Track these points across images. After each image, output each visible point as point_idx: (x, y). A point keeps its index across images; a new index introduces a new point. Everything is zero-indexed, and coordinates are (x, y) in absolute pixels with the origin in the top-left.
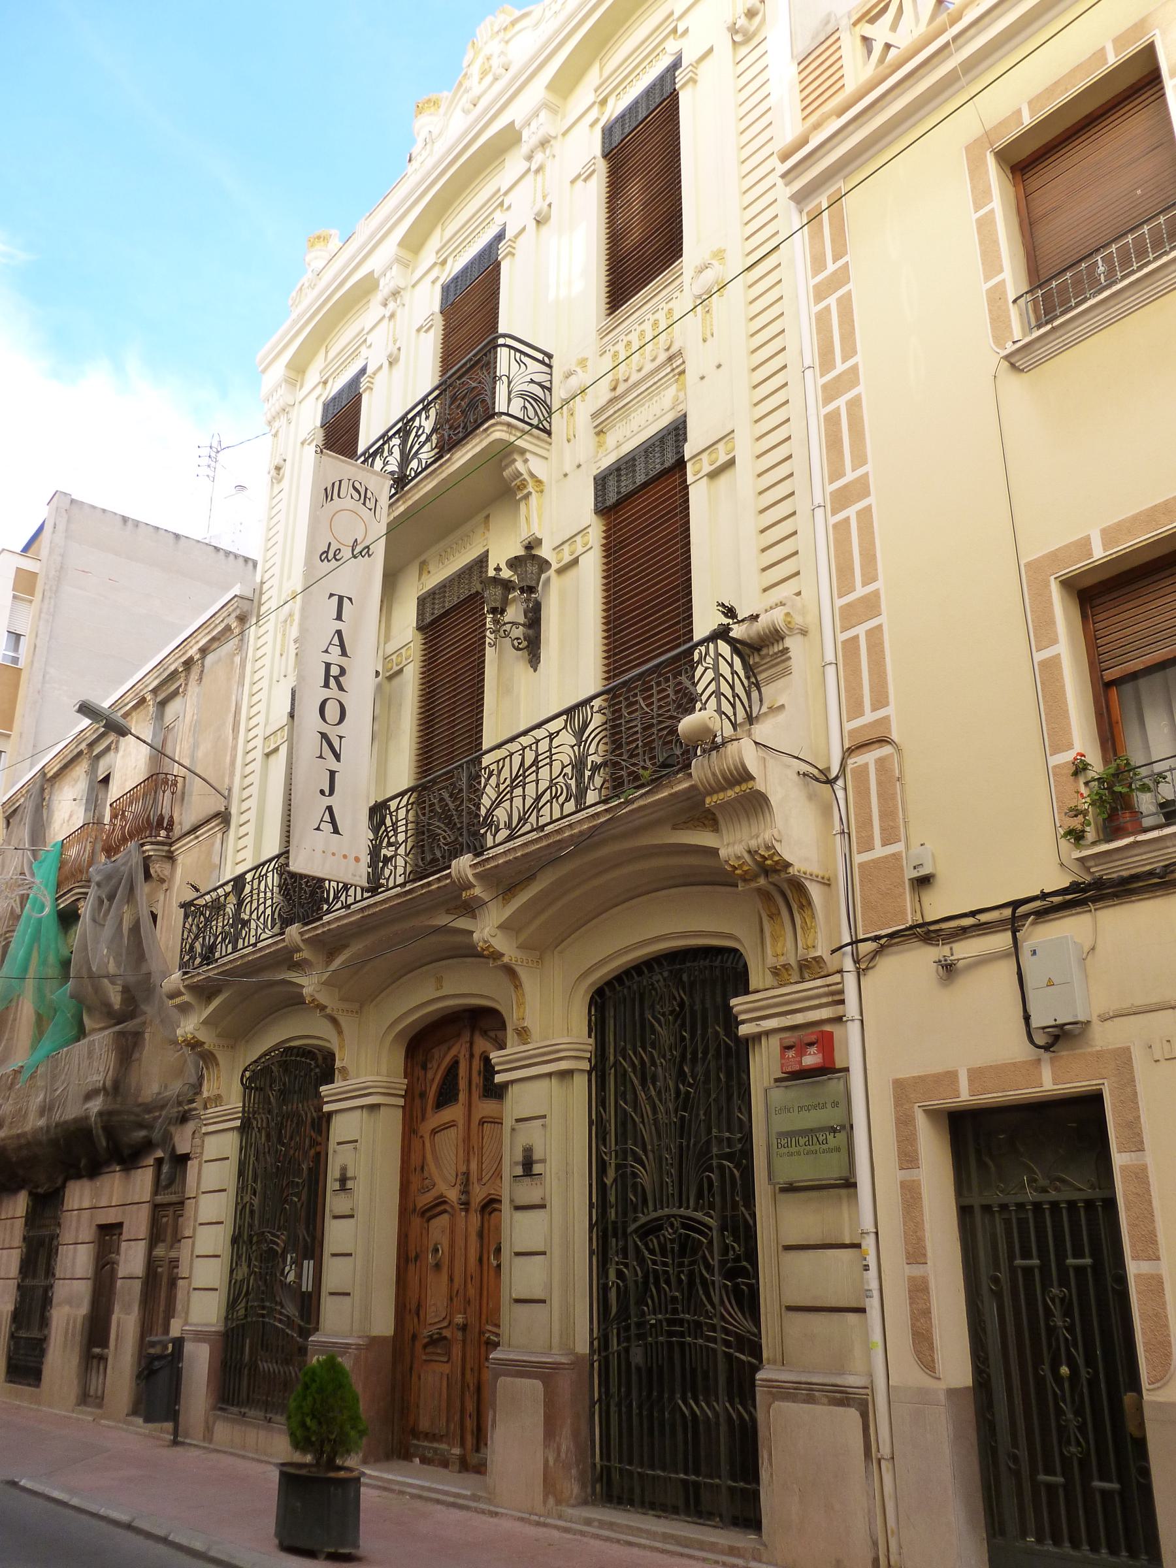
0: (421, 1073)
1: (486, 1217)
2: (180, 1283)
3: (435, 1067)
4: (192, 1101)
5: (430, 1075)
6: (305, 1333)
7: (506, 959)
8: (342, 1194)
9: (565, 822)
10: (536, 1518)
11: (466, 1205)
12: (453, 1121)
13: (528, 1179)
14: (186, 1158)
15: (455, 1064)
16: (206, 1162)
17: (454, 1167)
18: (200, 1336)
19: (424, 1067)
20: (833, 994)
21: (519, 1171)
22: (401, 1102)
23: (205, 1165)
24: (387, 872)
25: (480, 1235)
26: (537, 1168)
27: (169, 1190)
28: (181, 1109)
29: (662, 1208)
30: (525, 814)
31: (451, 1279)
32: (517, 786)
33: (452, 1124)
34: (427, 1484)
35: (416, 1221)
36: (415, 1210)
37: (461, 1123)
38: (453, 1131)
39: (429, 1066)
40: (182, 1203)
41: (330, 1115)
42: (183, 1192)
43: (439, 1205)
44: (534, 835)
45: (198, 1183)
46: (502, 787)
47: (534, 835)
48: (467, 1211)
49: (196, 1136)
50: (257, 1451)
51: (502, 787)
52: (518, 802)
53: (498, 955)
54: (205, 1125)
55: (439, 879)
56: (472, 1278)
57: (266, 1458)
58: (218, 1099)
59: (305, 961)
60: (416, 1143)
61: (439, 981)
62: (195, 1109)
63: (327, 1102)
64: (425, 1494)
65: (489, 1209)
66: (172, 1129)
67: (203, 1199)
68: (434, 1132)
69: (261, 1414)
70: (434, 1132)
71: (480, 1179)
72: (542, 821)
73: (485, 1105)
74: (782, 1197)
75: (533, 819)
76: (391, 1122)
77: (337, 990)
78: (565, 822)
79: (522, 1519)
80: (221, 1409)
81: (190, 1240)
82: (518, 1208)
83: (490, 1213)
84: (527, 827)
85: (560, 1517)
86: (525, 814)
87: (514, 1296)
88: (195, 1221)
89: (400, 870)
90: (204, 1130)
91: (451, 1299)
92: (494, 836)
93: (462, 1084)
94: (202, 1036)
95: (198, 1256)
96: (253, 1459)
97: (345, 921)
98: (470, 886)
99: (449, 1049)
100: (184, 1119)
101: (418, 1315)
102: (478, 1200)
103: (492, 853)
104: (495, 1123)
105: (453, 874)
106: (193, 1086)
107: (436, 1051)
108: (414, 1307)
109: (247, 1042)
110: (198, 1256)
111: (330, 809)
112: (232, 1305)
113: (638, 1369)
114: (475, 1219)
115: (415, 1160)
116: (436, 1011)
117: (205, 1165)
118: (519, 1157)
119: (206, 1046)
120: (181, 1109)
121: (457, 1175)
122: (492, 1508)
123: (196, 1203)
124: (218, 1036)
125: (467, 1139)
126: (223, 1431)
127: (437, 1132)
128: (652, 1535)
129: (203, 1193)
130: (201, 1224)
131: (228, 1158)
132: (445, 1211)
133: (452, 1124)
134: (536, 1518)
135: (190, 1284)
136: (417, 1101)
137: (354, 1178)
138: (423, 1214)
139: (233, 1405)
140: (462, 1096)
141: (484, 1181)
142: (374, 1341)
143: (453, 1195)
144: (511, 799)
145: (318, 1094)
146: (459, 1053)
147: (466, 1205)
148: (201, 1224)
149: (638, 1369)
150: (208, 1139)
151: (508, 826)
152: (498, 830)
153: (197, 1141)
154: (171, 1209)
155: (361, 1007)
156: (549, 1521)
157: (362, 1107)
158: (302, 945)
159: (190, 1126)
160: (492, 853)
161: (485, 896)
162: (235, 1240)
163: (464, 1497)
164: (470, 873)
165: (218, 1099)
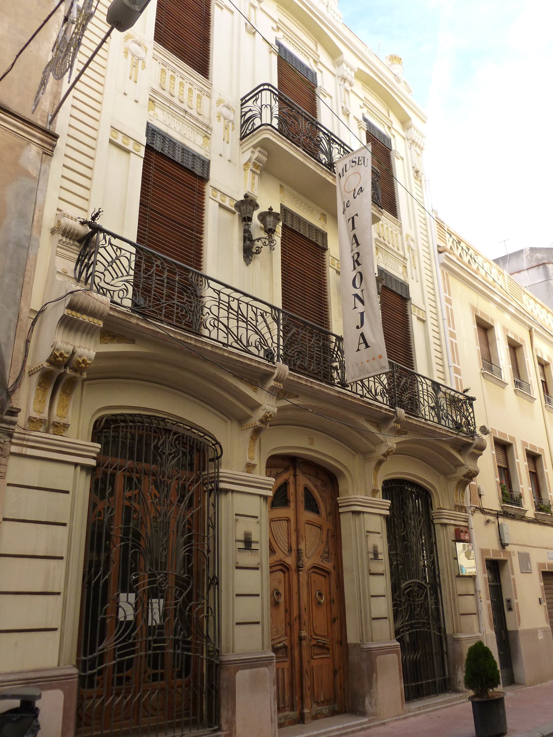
8: (248, 552)
10: (401, 716)
17: (287, 545)
20: (465, 519)
21: (372, 556)
26: (254, 546)
29: (409, 580)
34: (341, 726)
55: (306, 381)
56: (305, 610)
64: (344, 731)
74: (457, 578)
79: (396, 720)
82: (371, 574)
85: (409, 712)
87: (373, 616)
93: (292, 498)
111: (362, 335)
113: (408, 644)
118: (371, 549)
122: (382, 722)
128: (440, 703)
134: (401, 716)
137: (257, 542)
140: (292, 505)
146: (289, 478)
149: (408, 644)
156: (407, 715)
162: (215, 581)
163: (365, 723)
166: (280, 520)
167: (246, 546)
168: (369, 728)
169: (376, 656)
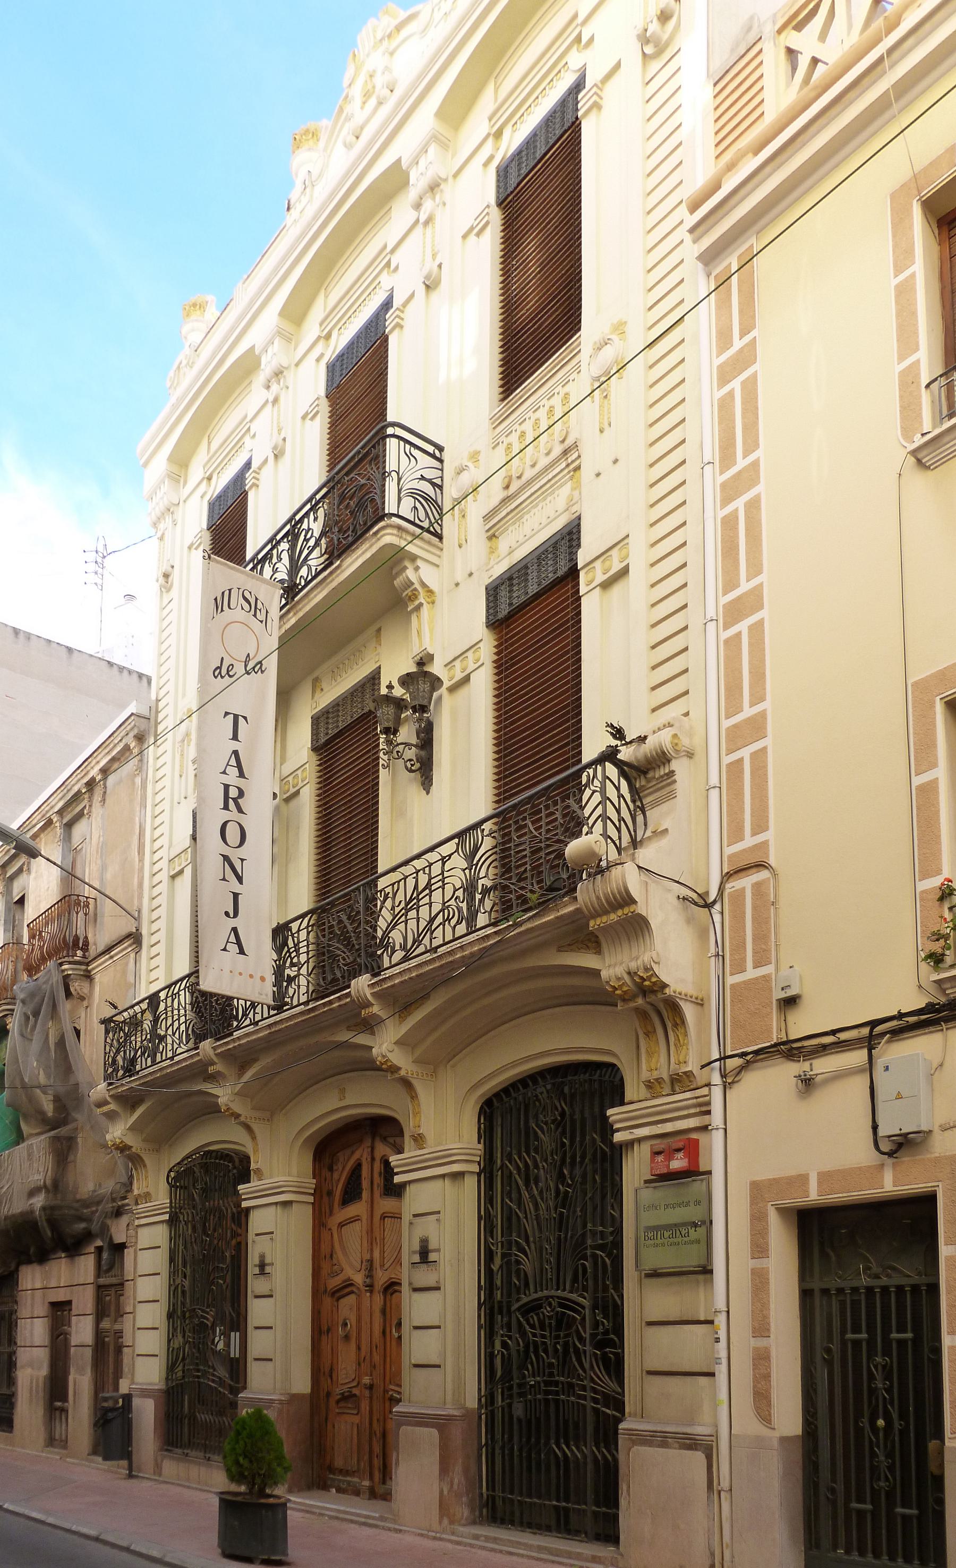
0: (328, 1174)
1: (388, 1297)
2: (125, 1350)
3: (341, 1169)
4: (125, 1198)
5: (336, 1175)
6: (235, 1391)
7: (403, 1073)
8: (262, 1277)
9: (456, 944)
11: (370, 1287)
12: (358, 1216)
13: (425, 1266)
14: (122, 1247)
15: (358, 1166)
16: (140, 1250)
17: (359, 1255)
18: (145, 1393)
19: (331, 1169)
21: (417, 1258)
22: (311, 1199)
23: (139, 1253)
24: (291, 991)
25: (383, 1312)
27: (110, 1274)
28: (115, 1204)
30: (419, 935)
31: (359, 1348)
32: (411, 909)
33: (356, 1219)
34: (342, 1508)
35: (327, 1301)
36: (325, 1291)
37: (364, 1218)
38: (357, 1226)
39: (335, 1168)
40: (122, 1284)
41: (248, 1210)
42: (123, 1275)
43: (347, 1287)
44: (428, 957)
45: (135, 1268)
46: (397, 910)
47: (428, 957)
48: (371, 1292)
49: (130, 1227)
50: (199, 1483)
51: (397, 910)
52: (412, 924)
53: (394, 1069)
54: (138, 1218)
55: (339, 998)
56: (376, 1347)
57: (208, 1488)
58: (147, 1196)
59: (219, 1073)
60: (325, 1235)
61: (342, 1092)
62: (128, 1205)
63: (245, 1199)
64: (341, 1516)
65: (391, 1291)
66: (109, 1222)
67: (141, 1282)
68: (341, 1225)
69: (201, 1454)
70: (341, 1225)
71: (382, 1266)
72: (436, 943)
73: (385, 1202)
75: (426, 941)
76: (302, 1218)
77: (249, 1100)
78: (456, 944)
80: (167, 1450)
81: (131, 1316)
82: (416, 1290)
83: (392, 1294)
84: (421, 949)
86: (419, 935)
87: (413, 1362)
88: (135, 1299)
89: (303, 989)
90: (137, 1222)
91: (359, 1364)
92: (391, 957)
93: (365, 1184)
94: (129, 1141)
95: (139, 1329)
96: (196, 1489)
97: (254, 1037)
98: (369, 1005)
99: (353, 1153)
100: (118, 1213)
101: (331, 1377)
102: (381, 1283)
103: (388, 973)
104: (395, 1217)
105: (353, 993)
106: (124, 1184)
107: (340, 1154)
108: (327, 1371)
109: (170, 1146)
110: (139, 1329)
112: (171, 1368)
114: (378, 1299)
115: (325, 1249)
116: (340, 1118)
117: (139, 1253)
119: (134, 1150)
120: (115, 1204)
121: (362, 1262)
123: (135, 1284)
124: (143, 1141)
125: (370, 1231)
126: (170, 1467)
127: (344, 1225)
129: (140, 1276)
130: (140, 1302)
131: (159, 1247)
132: (352, 1292)
133: (356, 1219)
135: (134, 1351)
136: (326, 1199)
138: (333, 1294)
139: (177, 1447)
140: (365, 1195)
141: (386, 1267)
142: (294, 1398)
143: (359, 1279)
144: (406, 922)
145: (236, 1192)
146: (361, 1156)
147: (370, 1287)
148: (140, 1302)
150: (140, 1231)
151: (404, 947)
152: (393, 951)
153: (131, 1232)
154: (113, 1290)
155: (272, 1116)
157: (276, 1204)
158: (215, 1059)
159: (125, 1219)
160: (388, 973)
161: (383, 1014)
162: (170, 1316)
164: (368, 993)
165: (147, 1196)
166: (352, 1222)
167: (421, 1259)
168: (376, 1526)
169: (399, 1425)
